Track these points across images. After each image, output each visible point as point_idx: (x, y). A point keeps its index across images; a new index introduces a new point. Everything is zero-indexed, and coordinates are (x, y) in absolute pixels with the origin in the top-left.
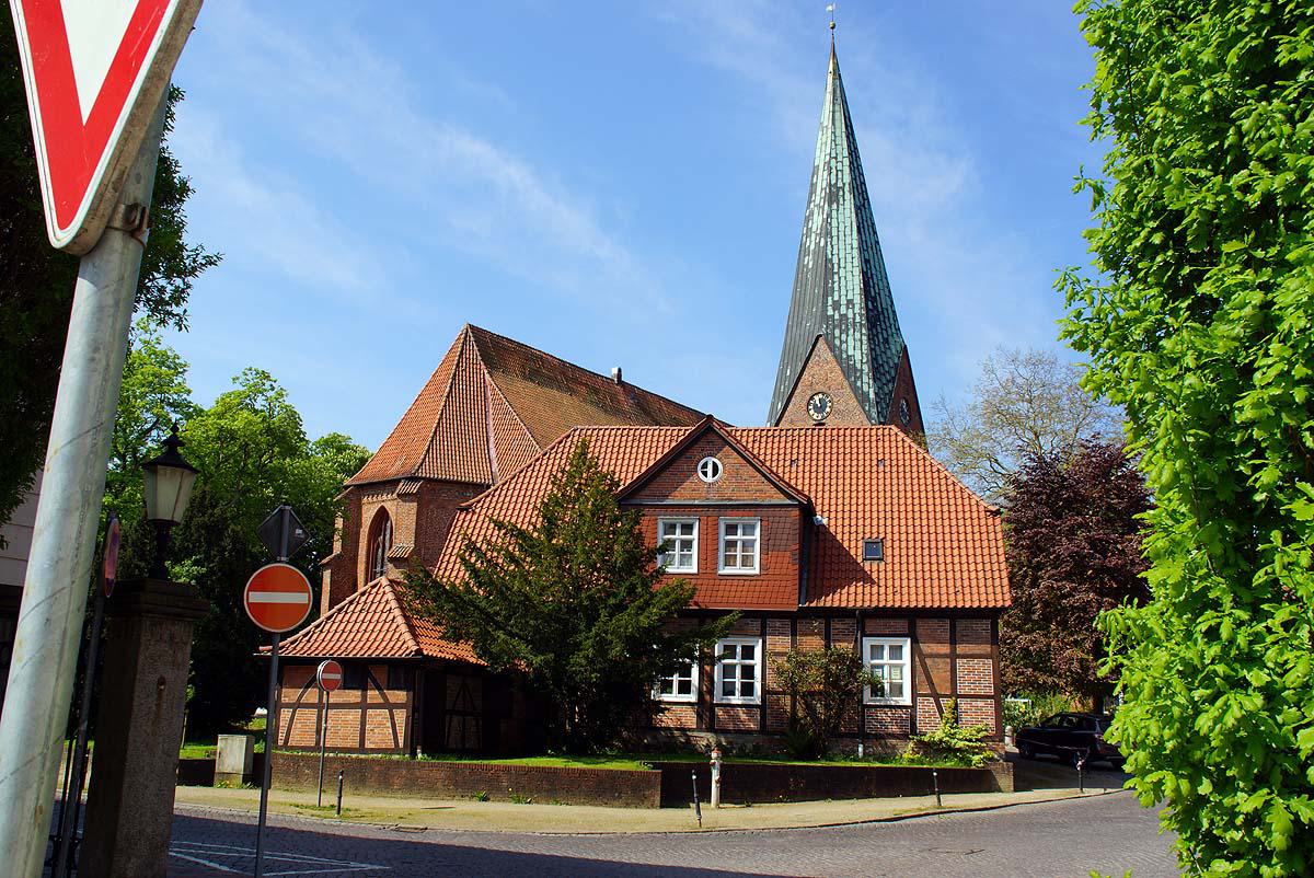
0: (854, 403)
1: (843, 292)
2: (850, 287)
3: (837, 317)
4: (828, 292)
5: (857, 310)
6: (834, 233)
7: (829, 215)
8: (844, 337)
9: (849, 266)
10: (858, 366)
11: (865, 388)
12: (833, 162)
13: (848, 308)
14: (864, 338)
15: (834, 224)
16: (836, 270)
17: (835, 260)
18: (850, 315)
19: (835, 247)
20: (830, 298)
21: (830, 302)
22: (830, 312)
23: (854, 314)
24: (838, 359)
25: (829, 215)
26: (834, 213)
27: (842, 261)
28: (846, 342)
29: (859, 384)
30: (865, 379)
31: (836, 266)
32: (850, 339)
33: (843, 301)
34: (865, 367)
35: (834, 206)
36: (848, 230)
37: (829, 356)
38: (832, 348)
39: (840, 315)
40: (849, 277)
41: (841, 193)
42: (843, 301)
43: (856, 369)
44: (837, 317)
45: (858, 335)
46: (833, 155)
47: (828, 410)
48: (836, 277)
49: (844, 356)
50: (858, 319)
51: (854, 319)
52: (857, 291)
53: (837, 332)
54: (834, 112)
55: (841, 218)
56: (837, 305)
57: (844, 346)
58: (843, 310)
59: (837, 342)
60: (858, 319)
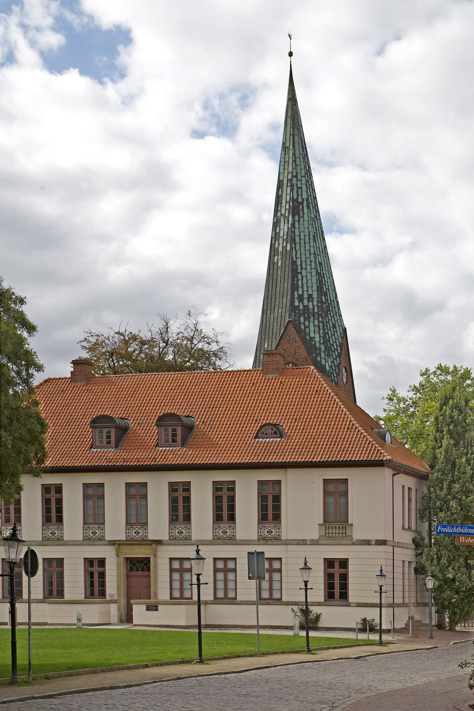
1: (305, 289)
2: (310, 285)
3: (301, 307)
4: (295, 287)
5: (315, 303)
6: (297, 241)
7: (293, 225)
8: (307, 323)
9: (309, 267)
10: (318, 345)
11: (323, 362)
12: (294, 180)
13: (309, 301)
14: (321, 324)
15: (297, 233)
16: (299, 271)
17: (299, 263)
18: (311, 307)
19: (298, 252)
20: (296, 293)
21: (296, 296)
22: (296, 303)
23: (314, 306)
26: (297, 224)
27: (304, 263)
28: (309, 327)
30: (323, 355)
31: (299, 267)
32: (311, 325)
33: (306, 296)
34: (322, 347)
36: (307, 241)
38: (299, 331)
39: (304, 306)
40: (309, 277)
41: (301, 207)
42: (306, 296)
44: (301, 307)
45: (316, 323)
46: (294, 174)
48: (300, 277)
49: (308, 338)
50: (316, 310)
51: (313, 309)
52: (315, 288)
53: (302, 319)
55: (302, 227)
56: (301, 298)
57: (307, 330)
59: (302, 327)
60: (316, 310)
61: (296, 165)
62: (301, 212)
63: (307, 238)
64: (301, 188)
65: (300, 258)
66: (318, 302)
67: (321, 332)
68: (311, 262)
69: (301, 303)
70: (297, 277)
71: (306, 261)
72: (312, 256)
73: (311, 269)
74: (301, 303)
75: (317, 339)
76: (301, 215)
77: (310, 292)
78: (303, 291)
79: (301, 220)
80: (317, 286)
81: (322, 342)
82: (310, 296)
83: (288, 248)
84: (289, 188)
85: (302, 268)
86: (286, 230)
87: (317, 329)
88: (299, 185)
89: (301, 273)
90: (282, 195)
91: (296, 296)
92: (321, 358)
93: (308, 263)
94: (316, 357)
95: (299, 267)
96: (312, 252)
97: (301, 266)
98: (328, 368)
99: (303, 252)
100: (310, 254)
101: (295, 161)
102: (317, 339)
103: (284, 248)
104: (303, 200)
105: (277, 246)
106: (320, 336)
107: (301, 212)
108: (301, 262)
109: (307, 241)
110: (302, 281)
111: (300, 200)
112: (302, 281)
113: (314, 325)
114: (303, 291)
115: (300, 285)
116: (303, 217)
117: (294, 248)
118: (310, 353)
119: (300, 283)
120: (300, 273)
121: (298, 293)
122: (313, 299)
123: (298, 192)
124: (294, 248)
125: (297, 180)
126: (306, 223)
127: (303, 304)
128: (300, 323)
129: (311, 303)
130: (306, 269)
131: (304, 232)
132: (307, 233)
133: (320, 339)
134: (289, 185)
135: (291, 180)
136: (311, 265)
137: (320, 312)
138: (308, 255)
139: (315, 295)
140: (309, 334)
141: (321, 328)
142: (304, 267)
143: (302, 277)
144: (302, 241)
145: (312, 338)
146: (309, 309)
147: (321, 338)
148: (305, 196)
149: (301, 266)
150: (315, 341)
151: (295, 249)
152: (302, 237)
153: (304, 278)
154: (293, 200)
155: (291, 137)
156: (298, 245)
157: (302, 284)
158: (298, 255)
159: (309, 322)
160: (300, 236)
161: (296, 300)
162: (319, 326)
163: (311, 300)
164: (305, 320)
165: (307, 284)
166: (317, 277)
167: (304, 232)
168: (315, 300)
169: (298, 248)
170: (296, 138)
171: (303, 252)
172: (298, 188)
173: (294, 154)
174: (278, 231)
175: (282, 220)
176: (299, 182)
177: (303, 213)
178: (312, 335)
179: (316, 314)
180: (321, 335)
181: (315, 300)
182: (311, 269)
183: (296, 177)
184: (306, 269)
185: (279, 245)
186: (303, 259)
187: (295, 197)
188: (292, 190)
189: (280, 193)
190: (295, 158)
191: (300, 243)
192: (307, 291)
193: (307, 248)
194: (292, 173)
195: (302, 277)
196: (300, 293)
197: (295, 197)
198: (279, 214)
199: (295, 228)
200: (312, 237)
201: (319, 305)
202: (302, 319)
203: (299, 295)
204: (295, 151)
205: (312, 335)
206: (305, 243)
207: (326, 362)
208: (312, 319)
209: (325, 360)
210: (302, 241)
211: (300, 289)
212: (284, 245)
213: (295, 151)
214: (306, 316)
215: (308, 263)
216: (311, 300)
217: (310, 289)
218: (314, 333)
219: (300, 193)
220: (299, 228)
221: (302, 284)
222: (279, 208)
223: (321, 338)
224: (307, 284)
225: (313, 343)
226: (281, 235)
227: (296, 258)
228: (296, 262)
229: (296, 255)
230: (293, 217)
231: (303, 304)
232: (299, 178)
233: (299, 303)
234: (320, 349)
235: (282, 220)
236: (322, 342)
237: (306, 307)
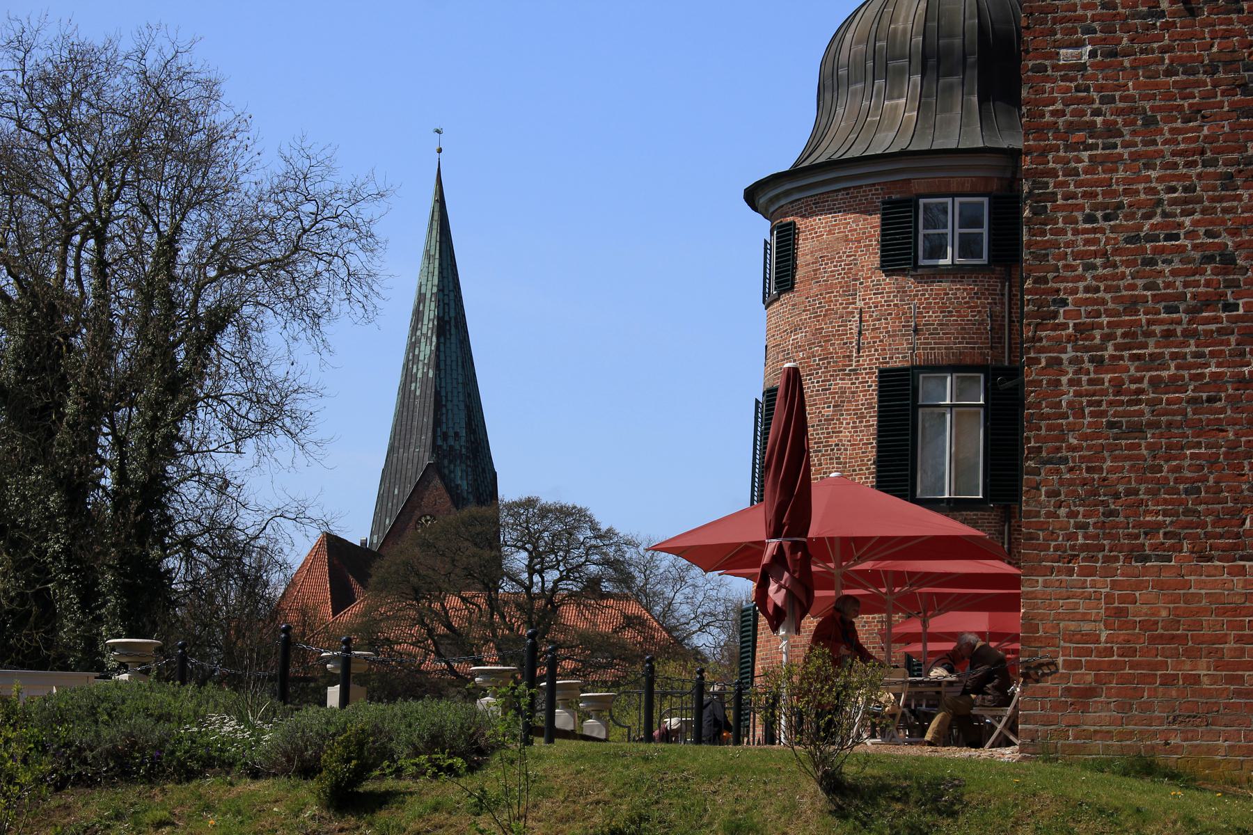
5: (463, 443)
8: (452, 466)
19: (443, 380)
22: (439, 442)
27: (449, 394)
33: (451, 433)
36: (454, 367)
42: (451, 433)
44: (445, 447)
53: (446, 462)
63: (454, 364)
64: (448, 304)
72: (460, 385)
79: (448, 341)
85: (447, 401)
86: (428, 352)
89: (445, 406)
93: (455, 394)
96: (460, 381)
97: (446, 397)
99: (449, 381)
100: (458, 383)
105: (415, 370)
109: (454, 367)
114: (448, 428)
126: (453, 346)
132: (454, 358)
142: (449, 398)
143: (447, 411)
144: (448, 368)
152: (448, 362)
156: (443, 372)
158: (443, 385)
171: (449, 381)
174: (417, 353)
177: (450, 334)
178: (459, 482)
186: (449, 389)
193: (455, 376)
195: (447, 411)
196: (444, 430)
200: (460, 363)
202: (446, 462)
210: (448, 368)
211: (444, 426)
215: (455, 394)
226: (421, 358)
232: (446, 292)
235: (423, 340)
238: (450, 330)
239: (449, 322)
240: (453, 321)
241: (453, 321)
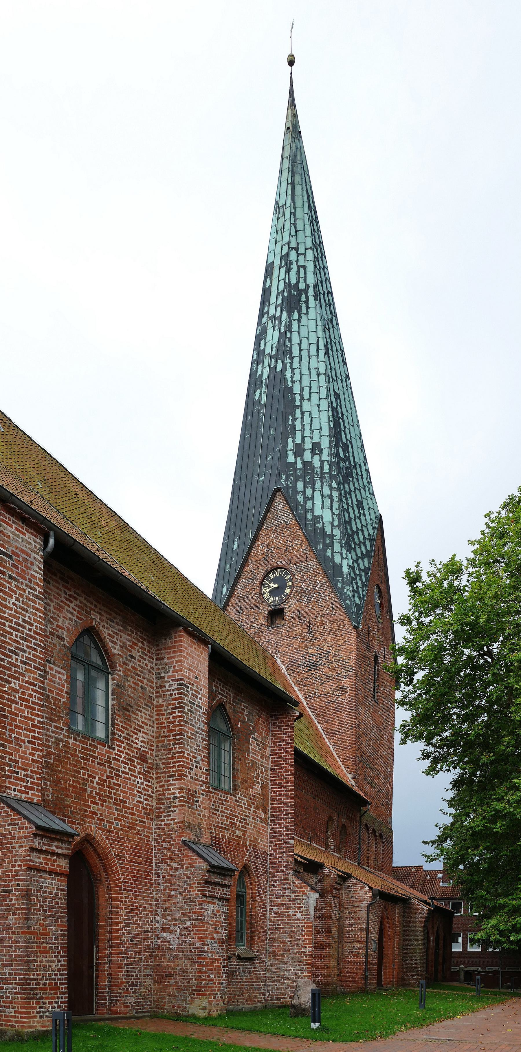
0: (321, 579)
1: (307, 433)
2: (316, 426)
3: (299, 465)
5: (325, 457)
6: (295, 352)
8: (309, 492)
9: (315, 397)
10: (328, 530)
11: (337, 559)
13: (313, 454)
14: (335, 494)
15: (295, 339)
16: (297, 403)
17: (297, 389)
18: (317, 463)
19: (297, 372)
20: (290, 440)
21: (290, 446)
22: (291, 458)
23: (322, 462)
24: (301, 521)
25: (289, 327)
26: (295, 326)
27: (306, 391)
28: (312, 498)
29: (329, 553)
30: (337, 547)
31: (298, 397)
32: (317, 494)
33: (308, 445)
34: (337, 532)
35: (295, 316)
36: (313, 352)
37: (289, 518)
38: (292, 505)
41: (303, 298)
42: (308, 445)
43: (324, 535)
44: (299, 465)
45: (326, 490)
46: (293, 244)
47: (287, 591)
48: (298, 413)
49: (310, 517)
50: (327, 469)
51: (322, 468)
52: (325, 431)
53: (300, 485)
54: (293, 184)
55: (304, 333)
56: (299, 450)
57: (309, 504)
58: (308, 456)
59: (300, 498)
60: (327, 469)
61: (297, 231)
62: (304, 306)
63: (313, 348)
64: (304, 267)
65: (300, 381)
66: (330, 455)
67: (336, 506)
68: (319, 387)
69: (299, 458)
70: (293, 414)
71: (310, 387)
72: (322, 378)
73: (320, 399)
74: (299, 458)
75: (327, 518)
76: (304, 310)
77: (316, 439)
78: (303, 438)
79: (304, 318)
80: (330, 428)
81: (336, 523)
82: (316, 446)
83: (279, 368)
84: (283, 270)
85: (302, 399)
86: (276, 339)
87: (327, 501)
88: (301, 263)
89: (300, 407)
90: (270, 287)
91: (290, 446)
92: (333, 549)
93: (315, 389)
94: (324, 550)
95: (298, 397)
96: (322, 370)
97: (301, 394)
98: (345, 569)
99: (305, 371)
100: (318, 374)
101: (295, 224)
102: (327, 518)
103: (272, 370)
104: (307, 286)
105: (259, 372)
106: (333, 514)
107: (304, 306)
108: (302, 389)
109: (313, 352)
110: (302, 420)
111: (302, 286)
112: (302, 420)
113: (322, 495)
114: (303, 438)
115: (298, 427)
116: (307, 314)
117: (288, 365)
118: (311, 543)
119: (298, 424)
120: (298, 406)
121: (293, 441)
122: (321, 450)
123: (298, 273)
124: (288, 365)
125: (298, 255)
126: (312, 324)
127: (302, 459)
128: (297, 492)
129: (317, 458)
130: (309, 400)
131: (308, 338)
132: (313, 340)
133: (333, 519)
134: (283, 264)
135: (288, 254)
136: (319, 393)
137: (333, 473)
138: (314, 377)
139: (325, 443)
140: (313, 511)
141: (336, 499)
142: (306, 396)
143: (303, 413)
144: (304, 354)
145: (318, 517)
146: (314, 468)
147: (335, 517)
148: (311, 280)
149: (301, 394)
150: (323, 523)
151: (291, 366)
152: (305, 346)
153: (307, 415)
154: (288, 286)
155: (290, 186)
156: (296, 360)
157: (303, 426)
158: (297, 377)
159: (314, 491)
160: (300, 345)
161: (290, 454)
162: (331, 497)
163: (317, 452)
164: (305, 487)
165: (311, 425)
166: (330, 413)
167: (308, 338)
168: (326, 453)
169: (296, 364)
170: (298, 188)
171: (305, 371)
172: (298, 267)
173: (293, 214)
174: (262, 348)
175: (270, 325)
176: (301, 258)
177: (308, 308)
178: (318, 512)
179: (327, 475)
180: (334, 511)
181: (326, 453)
182: (320, 399)
183: (297, 249)
184: (309, 400)
185: (263, 368)
186: (305, 383)
187: (294, 281)
188: (288, 271)
189: (268, 285)
190: (296, 220)
191: (300, 357)
192: (311, 437)
193: (314, 364)
194: (289, 243)
195: (303, 413)
196: (298, 440)
197: (294, 281)
198: (265, 319)
199: (291, 332)
200: (322, 347)
201: (333, 460)
202: (300, 485)
203: (296, 445)
204: (295, 208)
205: (318, 512)
206: (309, 356)
207: (342, 558)
208: (318, 485)
209: (342, 554)
210: (304, 354)
211: (298, 436)
212: (272, 365)
213: (295, 208)
214: (308, 480)
215: (315, 389)
216: (317, 452)
217: (316, 433)
218: (322, 508)
219: (302, 275)
220: (299, 332)
221: (303, 426)
222: (266, 309)
223: (335, 517)
224: (311, 425)
225: (319, 526)
226: (268, 351)
227: (293, 382)
228: (291, 388)
229: (292, 377)
230: (289, 314)
231: (302, 459)
232: (302, 250)
233: (296, 457)
234: (332, 536)
235: (270, 325)
236: (336, 523)
237: (308, 466)
238: (307, 302)
239: (306, 291)
240: (311, 291)
241: (311, 291)
